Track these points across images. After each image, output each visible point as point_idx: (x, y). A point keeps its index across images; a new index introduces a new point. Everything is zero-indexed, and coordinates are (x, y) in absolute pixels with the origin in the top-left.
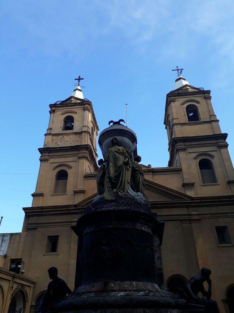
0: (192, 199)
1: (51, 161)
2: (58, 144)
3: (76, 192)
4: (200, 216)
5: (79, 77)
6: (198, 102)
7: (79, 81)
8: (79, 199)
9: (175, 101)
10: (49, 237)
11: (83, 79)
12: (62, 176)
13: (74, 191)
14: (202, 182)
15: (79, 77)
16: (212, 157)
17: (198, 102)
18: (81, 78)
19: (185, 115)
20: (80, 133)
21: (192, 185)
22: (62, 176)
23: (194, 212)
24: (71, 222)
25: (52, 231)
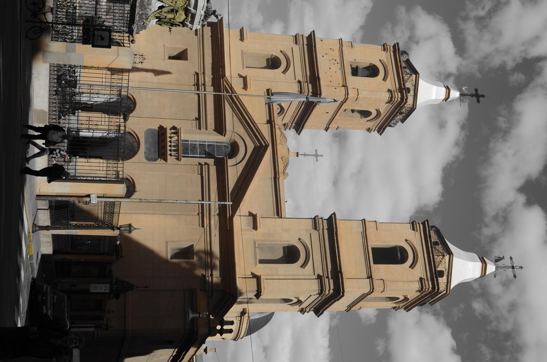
0: (231, 219)
1: (296, 48)
2: (326, 56)
3: (245, 79)
4: (208, 228)
5: (483, 96)
6: (412, 266)
7: (472, 95)
8: (237, 85)
9: (414, 229)
10: (186, 51)
11: (478, 101)
12: (273, 63)
13: (246, 76)
14: (258, 242)
15: (483, 96)
16: (304, 266)
17: (412, 266)
18: (481, 99)
19: (384, 242)
20: (345, 86)
21: (255, 227)
22: (273, 63)
23: (215, 221)
24: (204, 73)
25: (193, 54)
